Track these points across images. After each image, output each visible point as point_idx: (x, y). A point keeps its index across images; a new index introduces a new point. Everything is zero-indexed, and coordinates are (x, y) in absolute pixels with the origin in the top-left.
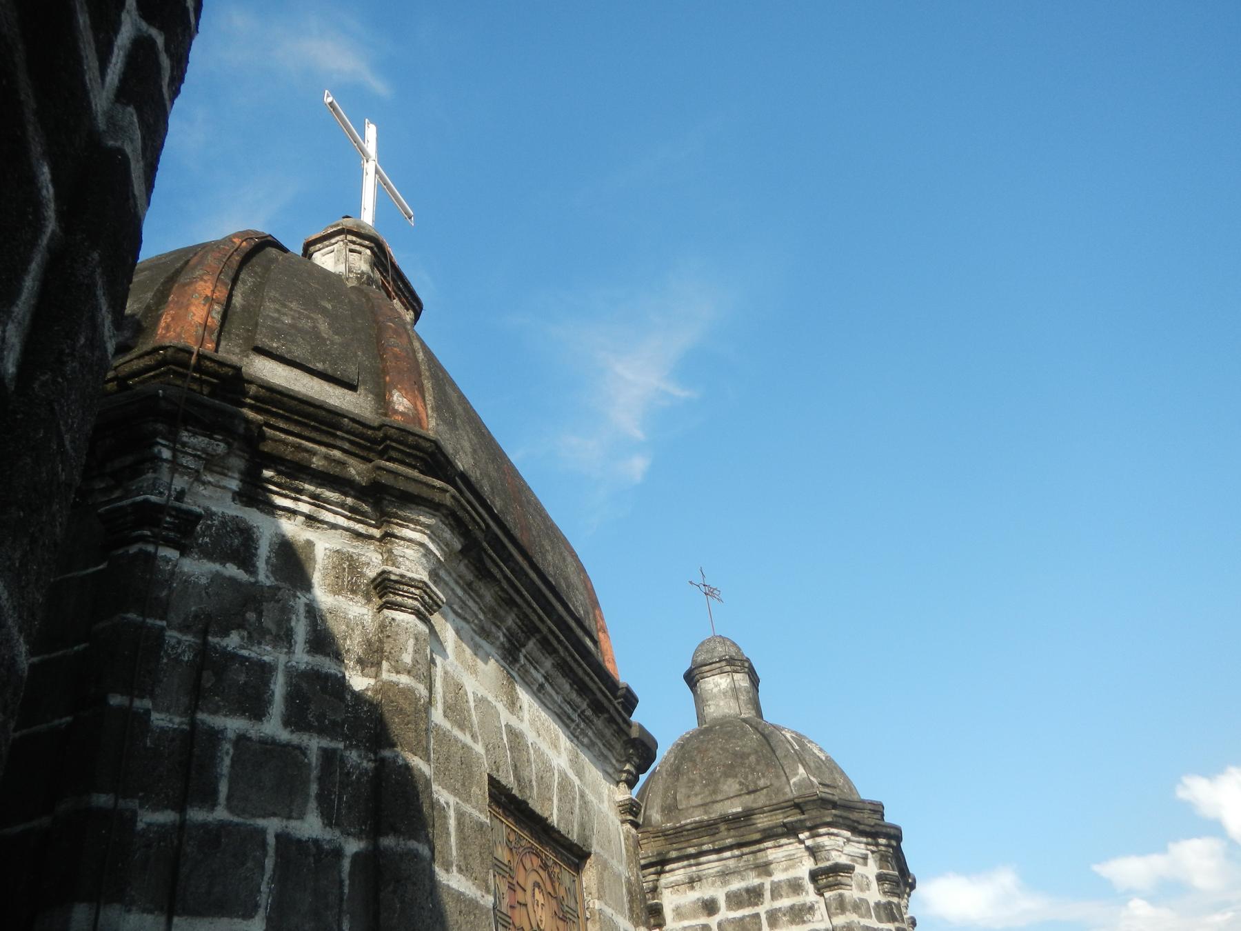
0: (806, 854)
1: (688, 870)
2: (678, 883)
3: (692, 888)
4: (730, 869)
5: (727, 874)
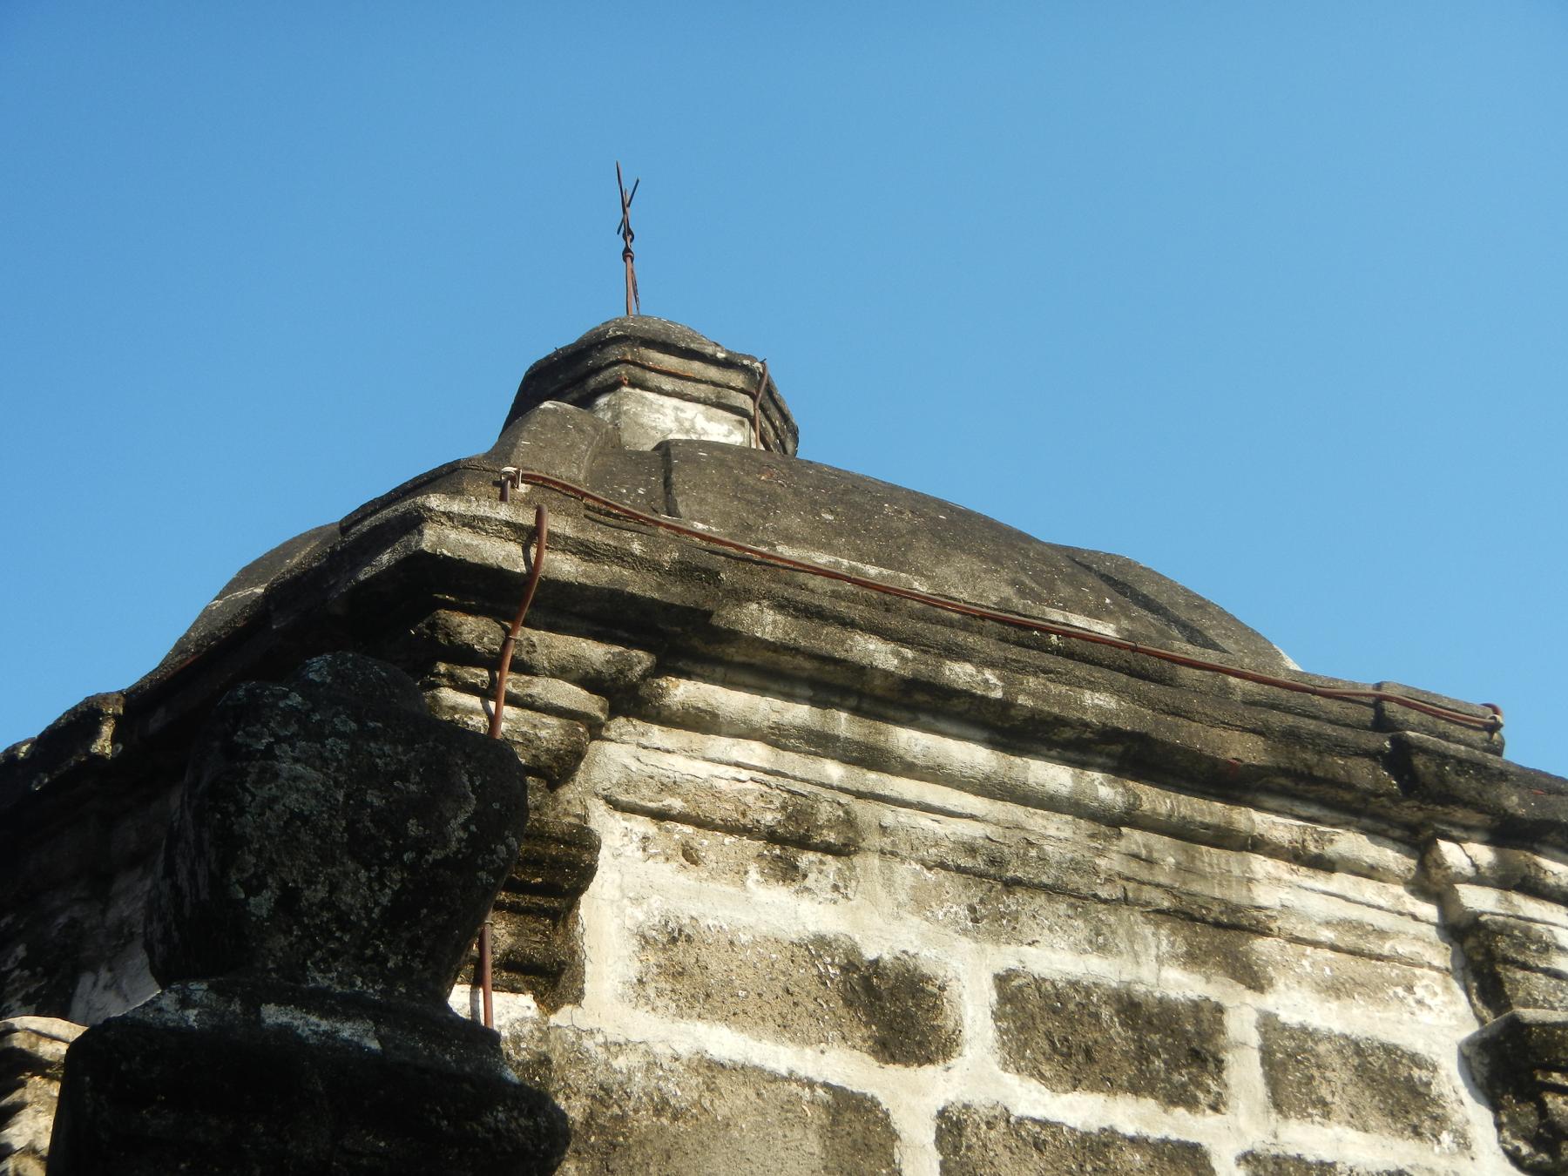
0: (1439, 955)
1: (793, 763)
2: (707, 808)
3: (787, 872)
4: (1043, 859)
5: (1012, 885)
